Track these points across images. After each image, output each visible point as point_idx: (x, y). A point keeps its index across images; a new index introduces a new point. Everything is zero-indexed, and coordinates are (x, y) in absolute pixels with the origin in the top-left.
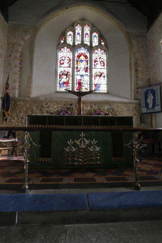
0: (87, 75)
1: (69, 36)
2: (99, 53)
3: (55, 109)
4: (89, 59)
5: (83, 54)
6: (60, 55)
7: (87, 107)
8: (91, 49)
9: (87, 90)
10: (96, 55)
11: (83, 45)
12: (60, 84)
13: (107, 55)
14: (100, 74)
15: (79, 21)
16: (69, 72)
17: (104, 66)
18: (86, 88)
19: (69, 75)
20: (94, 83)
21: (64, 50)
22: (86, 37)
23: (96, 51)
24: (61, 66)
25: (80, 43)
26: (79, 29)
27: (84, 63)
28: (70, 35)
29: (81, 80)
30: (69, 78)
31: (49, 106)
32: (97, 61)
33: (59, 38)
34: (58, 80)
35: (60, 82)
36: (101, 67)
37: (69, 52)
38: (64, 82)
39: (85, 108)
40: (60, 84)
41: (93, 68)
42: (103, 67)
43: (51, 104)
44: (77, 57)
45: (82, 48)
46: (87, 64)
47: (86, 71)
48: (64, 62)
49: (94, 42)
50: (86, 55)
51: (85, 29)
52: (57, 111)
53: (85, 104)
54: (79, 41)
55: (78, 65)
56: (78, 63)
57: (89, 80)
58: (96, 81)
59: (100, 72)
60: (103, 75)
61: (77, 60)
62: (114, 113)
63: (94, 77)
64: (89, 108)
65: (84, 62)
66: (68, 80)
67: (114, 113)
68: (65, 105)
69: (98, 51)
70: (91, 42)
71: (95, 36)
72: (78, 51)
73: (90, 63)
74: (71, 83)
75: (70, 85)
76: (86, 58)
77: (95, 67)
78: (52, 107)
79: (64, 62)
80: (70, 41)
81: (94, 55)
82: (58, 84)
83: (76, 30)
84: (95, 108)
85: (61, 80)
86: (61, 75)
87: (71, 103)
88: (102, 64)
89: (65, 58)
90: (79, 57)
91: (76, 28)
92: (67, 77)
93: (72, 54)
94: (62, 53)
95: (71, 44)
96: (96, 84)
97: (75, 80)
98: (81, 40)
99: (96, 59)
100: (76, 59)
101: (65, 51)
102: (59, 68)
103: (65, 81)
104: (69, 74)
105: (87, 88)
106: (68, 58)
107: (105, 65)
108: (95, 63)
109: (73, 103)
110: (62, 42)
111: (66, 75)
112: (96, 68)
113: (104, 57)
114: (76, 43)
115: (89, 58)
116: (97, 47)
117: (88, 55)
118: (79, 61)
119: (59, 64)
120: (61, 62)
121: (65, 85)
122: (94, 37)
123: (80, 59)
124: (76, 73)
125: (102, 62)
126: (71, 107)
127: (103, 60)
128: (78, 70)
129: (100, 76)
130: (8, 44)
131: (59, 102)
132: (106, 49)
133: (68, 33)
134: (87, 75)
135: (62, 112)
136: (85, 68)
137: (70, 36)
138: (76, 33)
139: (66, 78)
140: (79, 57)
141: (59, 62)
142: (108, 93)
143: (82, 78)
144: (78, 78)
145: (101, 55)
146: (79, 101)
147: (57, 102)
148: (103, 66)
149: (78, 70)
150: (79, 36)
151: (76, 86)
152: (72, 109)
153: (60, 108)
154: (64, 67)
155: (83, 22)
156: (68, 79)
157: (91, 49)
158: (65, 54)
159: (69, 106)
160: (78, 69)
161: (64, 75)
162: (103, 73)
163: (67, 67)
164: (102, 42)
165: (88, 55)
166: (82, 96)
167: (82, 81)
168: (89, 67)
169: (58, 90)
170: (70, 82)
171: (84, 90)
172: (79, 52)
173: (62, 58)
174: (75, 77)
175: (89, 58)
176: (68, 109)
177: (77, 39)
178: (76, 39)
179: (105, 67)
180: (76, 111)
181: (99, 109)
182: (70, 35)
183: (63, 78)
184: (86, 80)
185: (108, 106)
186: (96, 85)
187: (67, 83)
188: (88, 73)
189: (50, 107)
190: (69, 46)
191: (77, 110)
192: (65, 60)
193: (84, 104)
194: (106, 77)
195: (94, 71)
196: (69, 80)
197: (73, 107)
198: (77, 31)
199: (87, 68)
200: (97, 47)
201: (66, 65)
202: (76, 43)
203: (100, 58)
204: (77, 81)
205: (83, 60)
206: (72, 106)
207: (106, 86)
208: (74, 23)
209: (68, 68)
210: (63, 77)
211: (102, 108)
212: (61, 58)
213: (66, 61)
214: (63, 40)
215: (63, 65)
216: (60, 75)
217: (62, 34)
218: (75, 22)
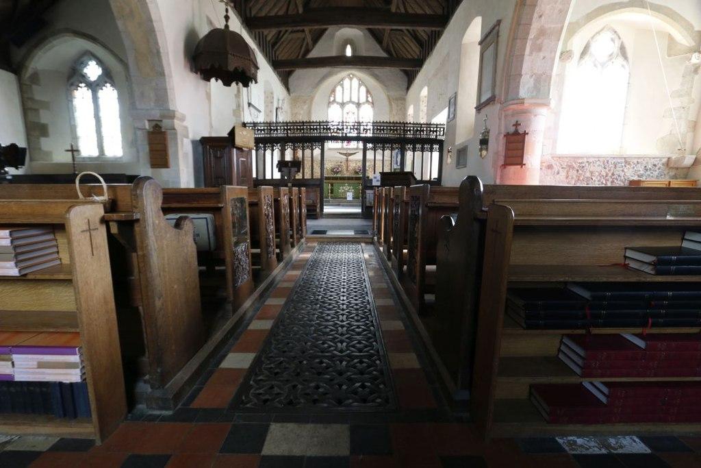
8: (358, 105)
11: (351, 102)
80: (339, 99)
110: (332, 99)
116: (364, 103)
130: (292, 115)
146: (347, 160)
157: (358, 105)
190: (338, 103)
200: (364, 103)
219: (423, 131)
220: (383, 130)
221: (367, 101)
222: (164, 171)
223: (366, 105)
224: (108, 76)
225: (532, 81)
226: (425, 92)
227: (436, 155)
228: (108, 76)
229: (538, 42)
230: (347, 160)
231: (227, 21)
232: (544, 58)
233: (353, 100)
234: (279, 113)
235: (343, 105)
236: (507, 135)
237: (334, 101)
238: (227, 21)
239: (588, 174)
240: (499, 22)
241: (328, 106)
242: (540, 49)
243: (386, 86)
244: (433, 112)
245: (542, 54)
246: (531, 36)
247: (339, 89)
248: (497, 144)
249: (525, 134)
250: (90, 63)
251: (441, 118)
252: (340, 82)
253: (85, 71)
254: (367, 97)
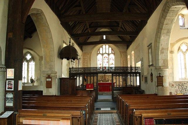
8: (109, 54)
11: (106, 53)
47: (107, 62)
80: (101, 52)
110: (98, 52)
116: (111, 54)
117: (108, 56)
124: (104, 64)
130: (83, 59)
138: (103, 49)
157: (109, 54)
158: (99, 57)
188: (108, 63)
190: (101, 54)
201: (100, 61)
213: (100, 59)
219: (133, 69)
220: (119, 69)
221: (112, 53)
222: (50, 89)
223: (112, 54)
224: (33, 59)
225: (162, 61)
226: (133, 52)
227: (138, 78)
228: (33, 59)
229: (163, 51)
231: (70, 43)
232: (165, 55)
233: (107, 52)
234: (79, 60)
235: (103, 54)
236: (157, 77)
237: (99, 53)
238: (70, 43)
239: (185, 87)
240: (151, 44)
241: (97, 55)
242: (163, 53)
243: (119, 48)
244: (136, 62)
245: (164, 54)
246: (160, 50)
247: (101, 49)
248: (155, 79)
249: (163, 77)
250: (28, 55)
251: (139, 64)
252: (102, 47)
253: (26, 57)
254: (112, 51)
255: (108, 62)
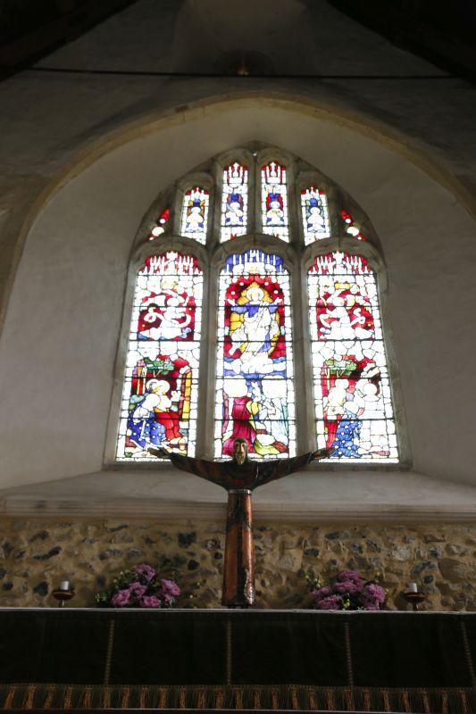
0: (284, 372)
1: (189, 207)
2: (339, 270)
3: (86, 566)
4: (287, 301)
5: (257, 278)
6: (145, 285)
7: (282, 554)
8: (296, 255)
9: (287, 450)
10: (324, 280)
11: (255, 239)
12: (136, 422)
13: (382, 277)
14: (353, 367)
15: (239, 152)
16: (187, 364)
17: (372, 327)
18: (276, 444)
19: (184, 379)
20: (319, 414)
21: (164, 264)
22: (269, 208)
23: (322, 264)
24: (145, 333)
25: (241, 231)
26: (236, 181)
27: (266, 317)
28: (197, 204)
29: (246, 399)
30: (183, 392)
31: (55, 552)
32: (332, 307)
33: (145, 219)
34: (125, 405)
35: (131, 412)
36: (350, 334)
37: (187, 271)
38: (155, 413)
39: (268, 558)
40: (136, 422)
41: (315, 337)
42: (368, 334)
43: (68, 536)
44: (229, 291)
45: (253, 254)
46: (281, 323)
47: (277, 354)
48: (160, 316)
49: (309, 225)
50: (274, 281)
51: (263, 180)
52: (100, 580)
53: (273, 537)
54: (237, 226)
55: (234, 326)
56: (235, 317)
57: (292, 397)
58: (333, 402)
59: (352, 358)
60: (367, 373)
61: (228, 308)
62: (455, 588)
63: (318, 382)
64: (296, 559)
65: (266, 312)
66: (179, 404)
67: (455, 588)
68: (148, 541)
69: (330, 265)
70: (296, 227)
71: (314, 204)
72: (232, 266)
73: (293, 316)
74: (194, 415)
75: (190, 426)
76: (273, 297)
77: (320, 333)
78: (70, 554)
79: (160, 316)
80: (193, 226)
81: (312, 281)
82: (124, 423)
83: (225, 186)
84: (330, 555)
85: (137, 405)
86: (141, 379)
87: (185, 531)
88: (361, 320)
89: (168, 297)
90: (237, 289)
91: (225, 178)
92: (173, 387)
93: (201, 279)
94: (154, 280)
95: (201, 238)
96: (332, 417)
97: (219, 398)
98: (245, 223)
99: (327, 296)
100: (222, 304)
101: (172, 269)
102: (132, 345)
103: (164, 405)
104: (182, 371)
105: (283, 440)
106: (182, 300)
107: (377, 323)
108: (322, 317)
109: (200, 527)
110: (158, 231)
111: (171, 377)
112: (328, 337)
113: (367, 287)
114: (225, 235)
115: (287, 293)
116: (325, 248)
117: (284, 281)
118: (239, 309)
119: (134, 326)
120: (146, 318)
121: (160, 428)
122: (311, 207)
123: (240, 302)
124: (221, 365)
125: (359, 310)
126: (182, 552)
127: (362, 302)
128: (232, 352)
129: (354, 377)
131: (115, 525)
132: (373, 252)
133: (187, 198)
134: (284, 372)
135: (126, 587)
136: (270, 341)
137: (196, 210)
138: (225, 198)
139: (169, 395)
140: (237, 289)
141: (136, 315)
142: (405, 467)
143: (257, 391)
144: (237, 388)
145: (351, 279)
147: (100, 523)
148: (366, 327)
149: (232, 352)
150: (235, 205)
151: (222, 433)
152: (193, 565)
153: (115, 562)
154: (160, 340)
155: (254, 155)
156: (176, 396)
157: (296, 255)
158: (167, 281)
159: (171, 549)
160: (235, 346)
161: (160, 377)
162: (366, 361)
163: (177, 339)
164: (351, 225)
165: (284, 281)
166: (254, 484)
167: (252, 407)
168: (288, 338)
169: (121, 455)
170: (191, 411)
171: (264, 451)
172: (238, 270)
173: (151, 301)
174: (219, 384)
175: (287, 293)
176: (168, 565)
177: (228, 220)
178: (223, 218)
179: (378, 333)
180: (215, 582)
181: (362, 562)
182: (197, 204)
183: (150, 391)
184: (277, 402)
185: (414, 544)
186: (331, 426)
187: (170, 419)
188: (288, 365)
189: (61, 555)
190: (187, 248)
191: (223, 571)
192: (166, 306)
193: (265, 536)
194: (385, 382)
195: (319, 355)
196: (186, 403)
197: (201, 552)
198: (226, 191)
199: (281, 339)
200: (325, 248)
201: (170, 328)
202: (225, 235)
203: (347, 292)
204: (225, 408)
205: (257, 307)
206: (194, 547)
207: (392, 426)
208: (213, 160)
209: (182, 345)
210: (154, 387)
211: (379, 560)
212: (146, 299)
213: (173, 311)
214: (160, 225)
215: (154, 333)
216: (136, 379)
217: (157, 202)
218: (218, 155)
230: (236, 512)
255: (292, 345)
